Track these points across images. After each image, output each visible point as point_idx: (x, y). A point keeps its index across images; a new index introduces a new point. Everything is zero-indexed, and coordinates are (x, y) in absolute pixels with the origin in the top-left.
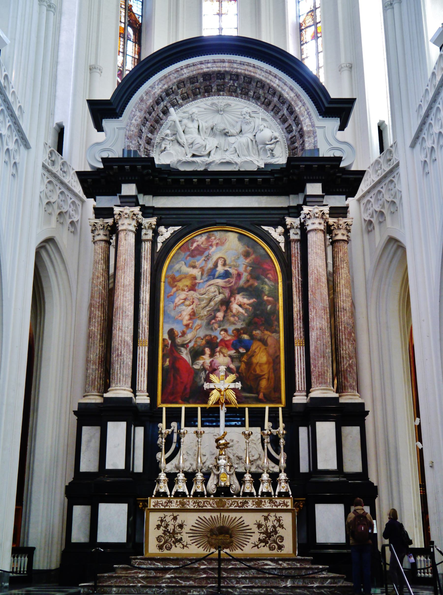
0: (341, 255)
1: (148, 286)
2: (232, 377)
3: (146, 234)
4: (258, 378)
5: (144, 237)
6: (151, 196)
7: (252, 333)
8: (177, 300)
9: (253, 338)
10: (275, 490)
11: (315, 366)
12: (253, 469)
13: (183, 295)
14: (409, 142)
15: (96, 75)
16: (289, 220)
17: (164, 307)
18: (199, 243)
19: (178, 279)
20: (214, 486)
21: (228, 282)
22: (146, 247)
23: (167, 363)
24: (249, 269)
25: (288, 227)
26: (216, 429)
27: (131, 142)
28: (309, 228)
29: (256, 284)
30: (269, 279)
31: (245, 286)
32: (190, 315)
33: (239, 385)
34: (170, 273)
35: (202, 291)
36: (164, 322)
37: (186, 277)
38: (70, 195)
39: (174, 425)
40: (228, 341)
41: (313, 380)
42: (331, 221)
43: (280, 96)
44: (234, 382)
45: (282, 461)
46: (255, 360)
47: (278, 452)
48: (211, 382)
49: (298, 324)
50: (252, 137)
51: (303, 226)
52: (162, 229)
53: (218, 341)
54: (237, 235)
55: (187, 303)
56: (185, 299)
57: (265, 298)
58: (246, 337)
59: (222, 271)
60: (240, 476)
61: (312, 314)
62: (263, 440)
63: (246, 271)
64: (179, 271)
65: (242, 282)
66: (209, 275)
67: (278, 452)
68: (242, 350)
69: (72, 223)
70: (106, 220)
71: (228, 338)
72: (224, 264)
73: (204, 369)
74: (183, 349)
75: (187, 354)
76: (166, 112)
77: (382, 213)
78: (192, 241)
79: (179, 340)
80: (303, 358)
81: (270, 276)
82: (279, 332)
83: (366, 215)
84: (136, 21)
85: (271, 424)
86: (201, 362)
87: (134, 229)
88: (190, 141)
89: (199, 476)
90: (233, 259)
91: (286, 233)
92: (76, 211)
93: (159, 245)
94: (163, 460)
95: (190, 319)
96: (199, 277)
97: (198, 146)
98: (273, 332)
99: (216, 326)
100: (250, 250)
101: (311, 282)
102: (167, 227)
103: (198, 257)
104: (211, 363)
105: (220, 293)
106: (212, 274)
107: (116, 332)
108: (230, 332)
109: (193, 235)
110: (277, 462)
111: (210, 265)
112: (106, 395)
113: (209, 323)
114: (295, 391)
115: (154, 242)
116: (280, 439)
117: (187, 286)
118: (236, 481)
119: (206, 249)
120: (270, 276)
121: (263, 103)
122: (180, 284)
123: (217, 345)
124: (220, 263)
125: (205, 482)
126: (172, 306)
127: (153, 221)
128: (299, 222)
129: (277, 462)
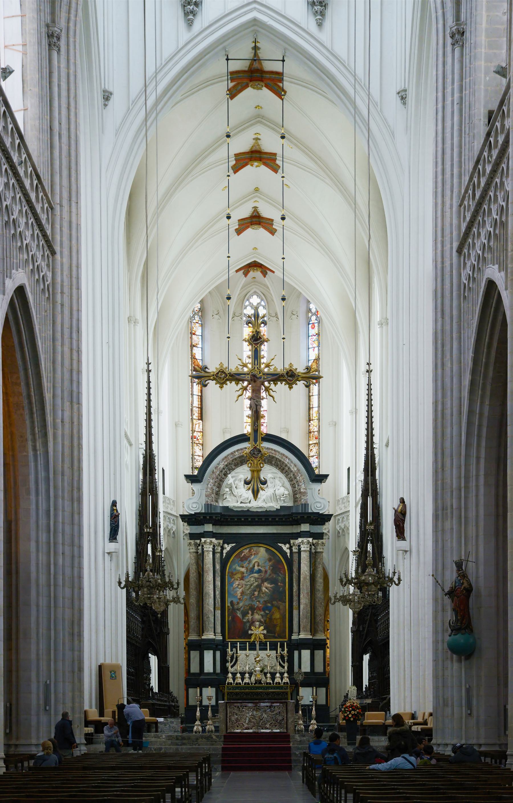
0: (319, 560)
1: (219, 578)
2: (262, 628)
3: (217, 549)
4: (275, 626)
5: (216, 551)
6: (219, 526)
7: (272, 602)
8: (234, 585)
9: (273, 605)
10: (282, 681)
11: (302, 623)
12: (272, 671)
16: (292, 541)
17: (228, 589)
18: (245, 553)
19: (234, 573)
20: (254, 680)
21: (261, 575)
22: (218, 556)
23: (230, 619)
24: (271, 568)
25: (292, 545)
27: (208, 499)
28: (302, 549)
29: (275, 576)
30: (281, 574)
31: (269, 577)
32: (241, 593)
34: (230, 571)
35: (247, 580)
36: (228, 597)
37: (238, 573)
38: (171, 517)
39: (234, 649)
40: (260, 607)
41: (301, 629)
42: (315, 541)
44: (263, 630)
45: (286, 668)
46: (273, 617)
47: (284, 663)
48: (252, 630)
49: (295, 598)
50: (273, 492)
51: (299, 546)
52: (226, 545)
53: (255, 607)
54: (265, 549)
55: (240, 587)
56: (238, 585)
57: (279, 584)
58: (269, 605)
59: (257, 569)
60: (265, 674)
61: (301, 596)
62: (277, 658)
63: (269, 569)
64: (235, 569)
65: (267, 575)
66: (250, 572)
67: (284, 663)
68: (267, 612)
70: (196, 541)
71: (260, 605)
72: (258, 566)
73: (248, 621)
74: (238, 611)
75: (240, 614)
77: (343, 530)
78: (242, 552)
79: (236, 607)
80: (297, 616)
81: (282, 572)
82: (286, 603)
83: (338, 526)
85: (281, 649)
86: (247, 618)
87: (211, 549)
88: (240, 495)
89: (247, 675)
90: (263, 562)
91: (290, 548)
92: (174, 524)
93: (224, 555)
94: (230, 667)
95: (241, 596)
96: (245, 573)
97: (244, 498)
98: (283, 602)
99: (254, 599)
100: (272, 558)
101: (302, 579)
102: (228, 544)
103: (245, 561)
104: (252, 618)
105: (256, 582)
108: (261, 602)
109: (242, 549)
110: (283, 667)
111: (251, 566)
113: (251, 598)
114: (293, 633)
115: (222, 553)
116: (284, 658)
117: (239, 578)
118: (264, 677)
119: (249, 557)
120: (282, 572)
122: (236, 577)
123: (255, 609)
124: (256, 565)
125: (250, 678)
126: (232, 588)
127: (221, 542)
128: (297, 543)
129: (283, 667)
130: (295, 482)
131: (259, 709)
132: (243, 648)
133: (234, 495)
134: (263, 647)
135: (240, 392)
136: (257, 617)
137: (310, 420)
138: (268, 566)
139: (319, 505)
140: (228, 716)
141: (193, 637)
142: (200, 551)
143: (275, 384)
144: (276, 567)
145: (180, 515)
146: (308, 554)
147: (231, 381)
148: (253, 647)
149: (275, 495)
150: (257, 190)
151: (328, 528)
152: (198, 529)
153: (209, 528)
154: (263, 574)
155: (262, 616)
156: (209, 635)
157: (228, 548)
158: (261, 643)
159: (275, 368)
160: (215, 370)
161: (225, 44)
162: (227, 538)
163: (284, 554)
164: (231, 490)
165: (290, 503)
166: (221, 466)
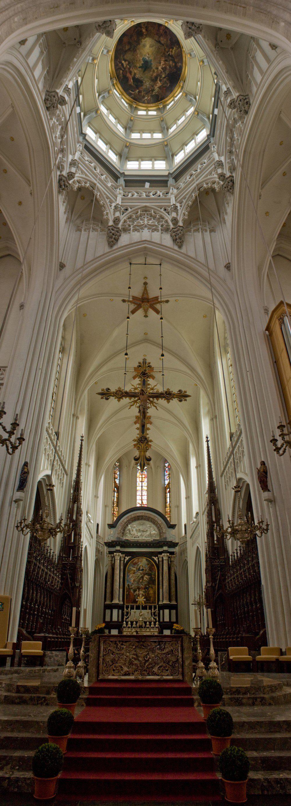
14: (189, 537)
22: (122, 562)
42: (170, 556)
51: (162, 558)
52: (126, 557)
69: (101, 552)
78: (134, 561)
91: (158, 559)
102: (127, 556)
115: (124, 561)
127: (124, 555)
130: (160, 528)
131: (143, 646)
138: (147, 568)
139: (172, 538)
140: (101, 655)
145: (105, 543)
146: (167, 561)
149: (150, 534)
151: (176, 550)
153: (118, 548)
157: (127, 558)
161: (130, 256)
163: (155, 562)
164: (130, 531)
166: (125, 521)
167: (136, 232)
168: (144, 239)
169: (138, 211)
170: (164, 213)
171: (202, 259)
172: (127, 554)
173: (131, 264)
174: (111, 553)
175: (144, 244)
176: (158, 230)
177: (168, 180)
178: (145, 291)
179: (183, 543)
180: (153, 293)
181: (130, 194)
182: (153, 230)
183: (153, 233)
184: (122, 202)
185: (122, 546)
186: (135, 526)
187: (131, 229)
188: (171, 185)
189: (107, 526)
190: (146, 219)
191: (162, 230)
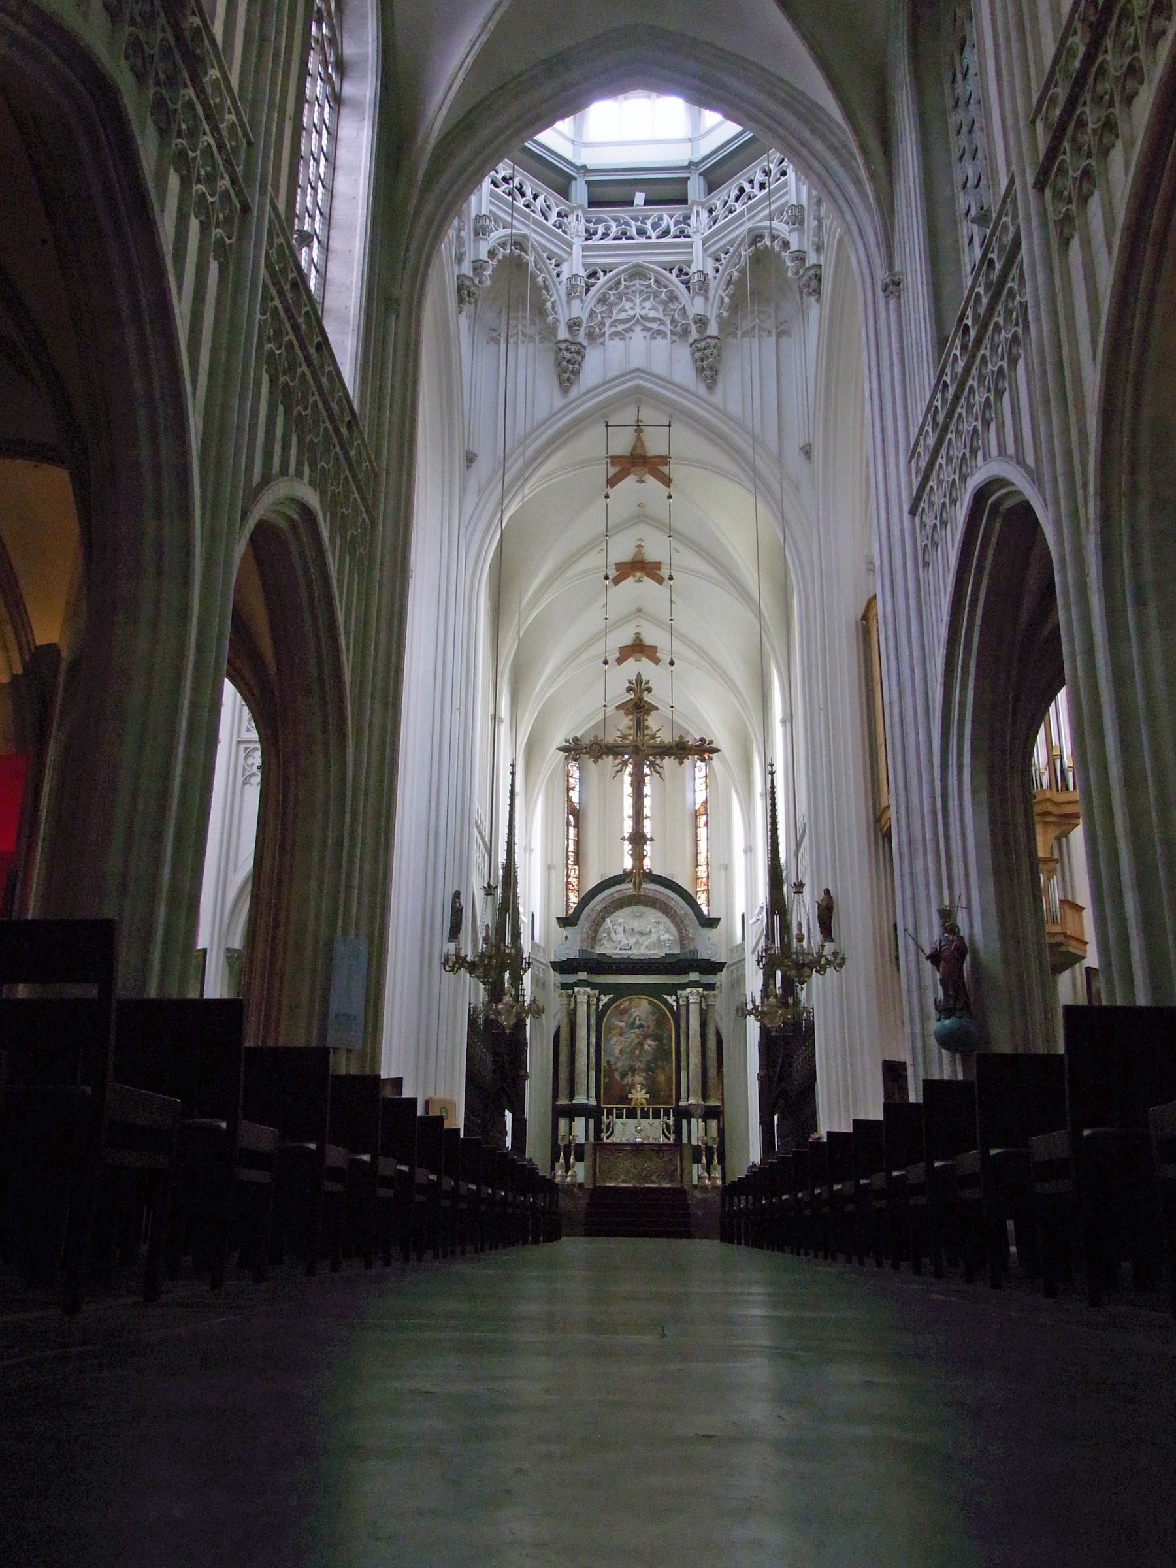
13: (615, 1039)
15: (553, 873)
22: (593, 1008)
26: (635, 1121)
33: (648, 1096)
42: (705, 993)
43: (675, 912)
46: (658, 1079)
47: (669, 1133)
49: (683, 1057)
52: (602, 997)
61: (691, 1055)
65: (650, 1032)
76: (604, 919)
78: (621, 1004)
79: (613, 1067)
84: (575, 808)
91: (677, 1001)
106: (632, 1026)
107: (577, 1065)
111: (632, 1020)
112: (574, 1102)
115: (598, 1005)
119: (630, 1009)
121: (664, 913)
127: (597, 992)
132: (619, 1116)
133: (612, 941)
134: (645, 1115)
135: (619, 767)
136: (638, 1079)
137: (697, 865)
138: (651, 1022)
139: (709, 952)
141: (564, 1101)
142: (572, 1006)
143: (662, 759)
144: (661, 1021)
146: (698, 1006)
147: (607, 754)
148: (631, 1114)
150: (639, 610)
151: (721, 978)
152: (571, 979)
153: (583, 976)
154: (645, 1030)
155: (645, 1078)
156: (580, 1099)
157: (605, 999)
158: (642, 1109)
159: (662, 741)
160: (588, 742)
162: (604, 989)
163: (670, 1006)
165: (677, 951)
167: (617, 339)
168: (633, 366)
169: (620, 279)
170: (677, 287)
171: (758, 431)
172: (604, 989)
173: (607, 426)
174: (564, 986)
175: (633, 379)
176: (665, 333)
177: (689, 178)
178: (639, 442)
179: (736, 963)
180: (655, 445)
181: (600, 226)
182: (653, 334)
183: (653, 341)
184: (583, 256)
185: (591, 971)
186: (621, 920)
187: (607, 334)
188: (694, 202)
189: (554, 921)
190: (638, 301)
191: (672, 333)
